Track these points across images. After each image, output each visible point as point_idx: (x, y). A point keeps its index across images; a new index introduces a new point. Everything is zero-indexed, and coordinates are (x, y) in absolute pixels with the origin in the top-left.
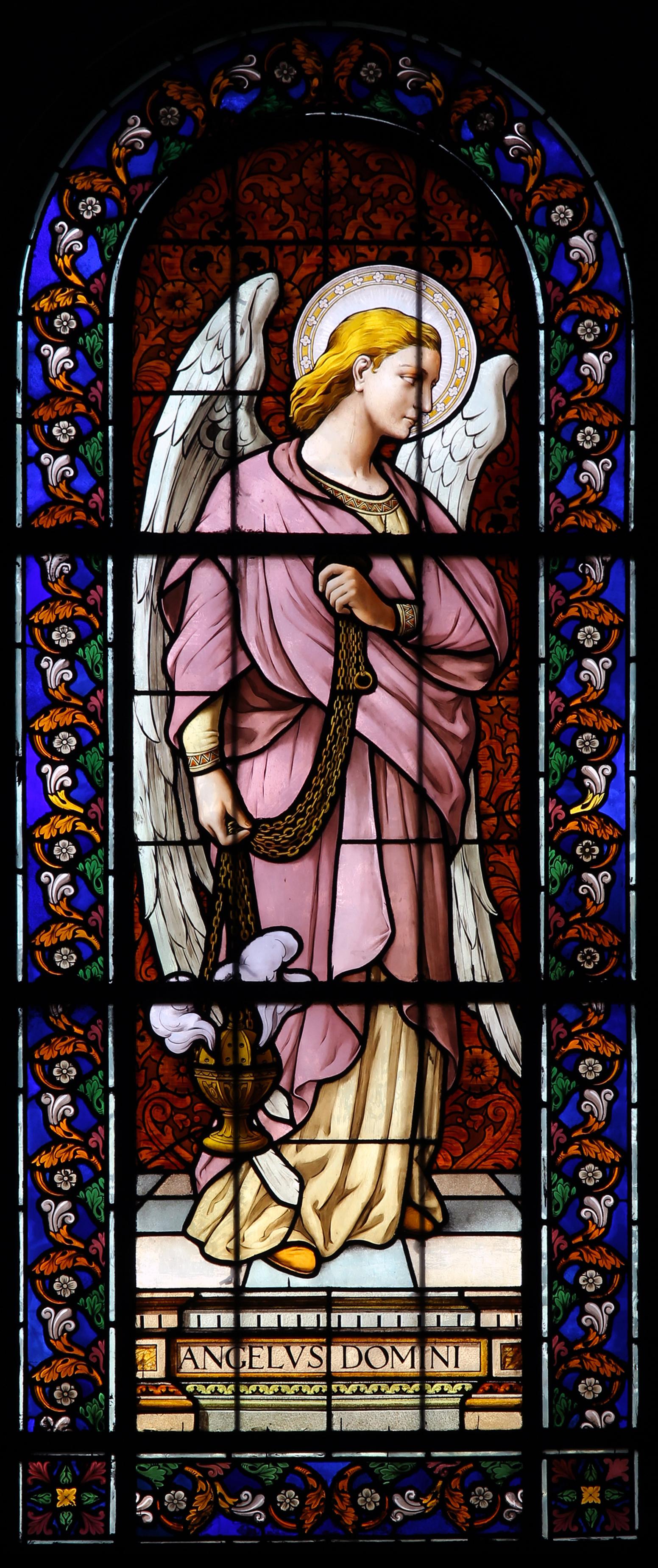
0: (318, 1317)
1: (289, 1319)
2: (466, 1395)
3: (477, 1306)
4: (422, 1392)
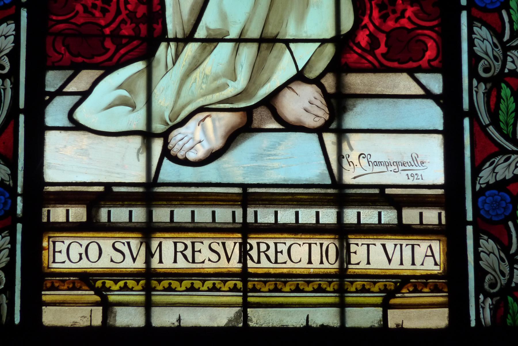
0: (234, 213)
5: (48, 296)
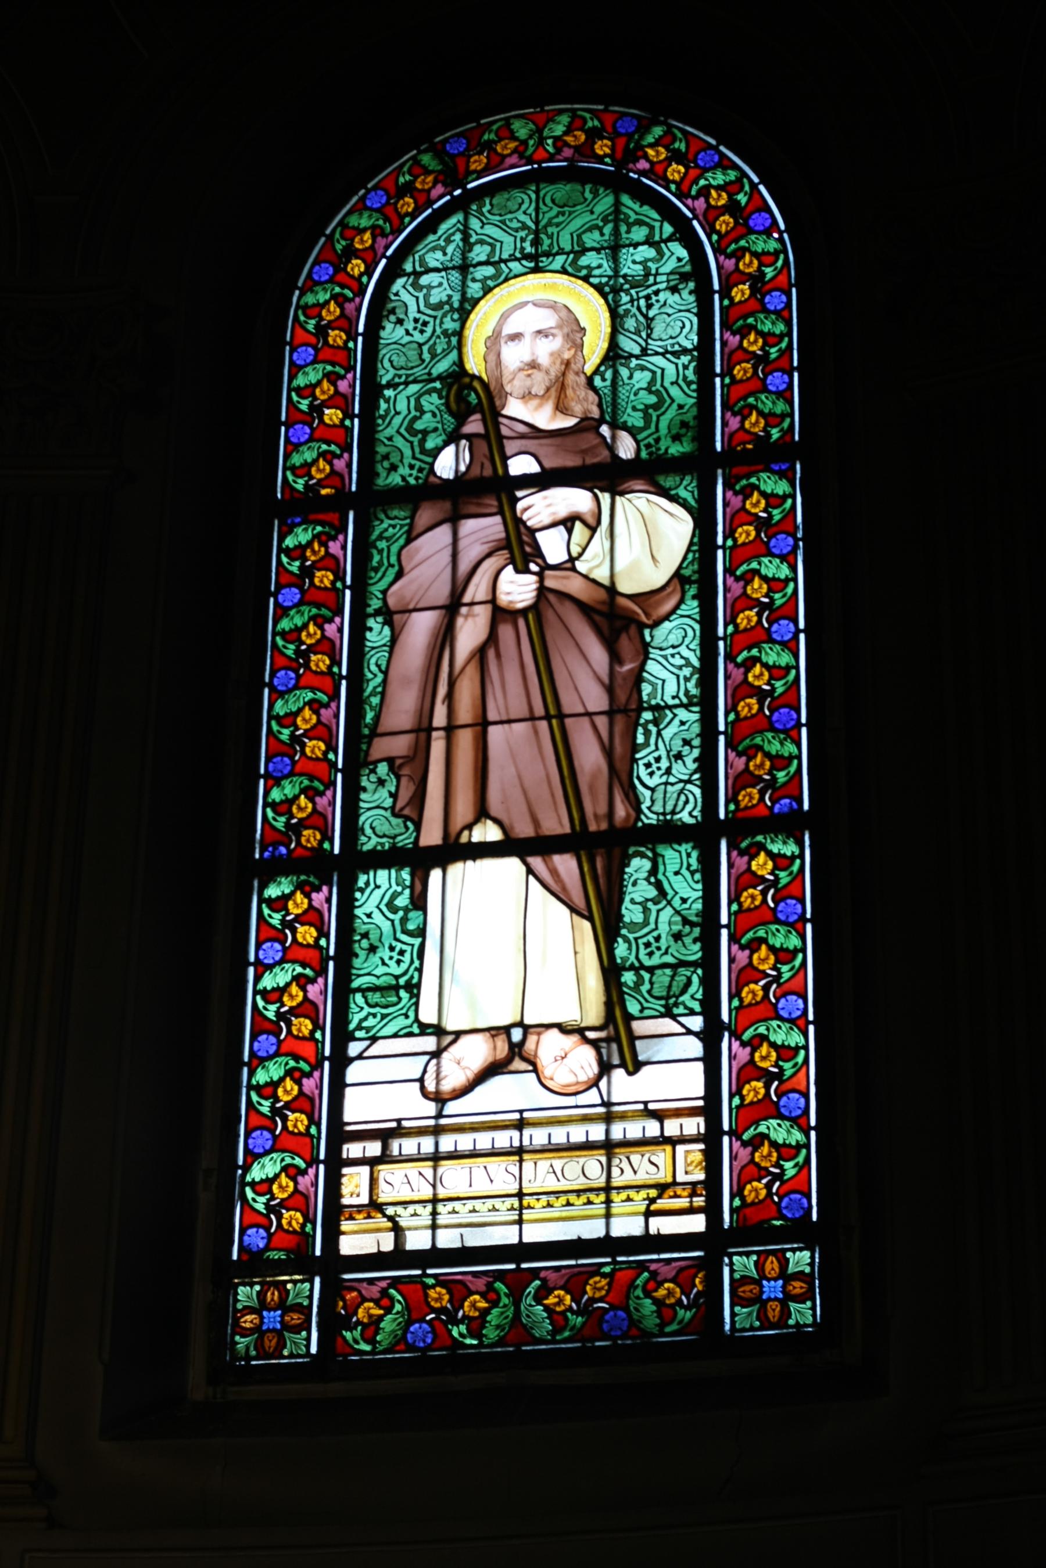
1: (484, 1141)
2: (652, 1201)
3: (659, 1116)
4: (608, 1202)
5: (346, 1226)
